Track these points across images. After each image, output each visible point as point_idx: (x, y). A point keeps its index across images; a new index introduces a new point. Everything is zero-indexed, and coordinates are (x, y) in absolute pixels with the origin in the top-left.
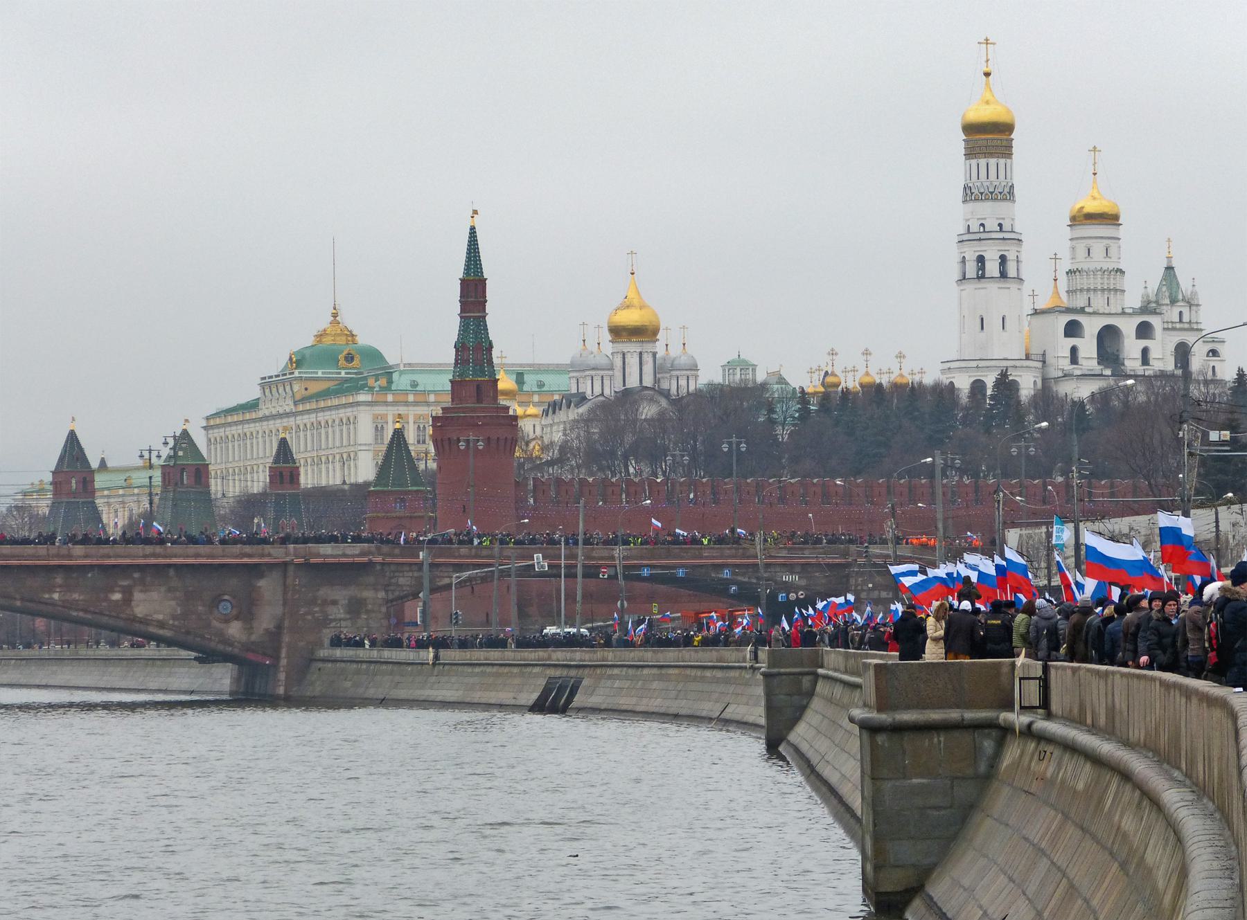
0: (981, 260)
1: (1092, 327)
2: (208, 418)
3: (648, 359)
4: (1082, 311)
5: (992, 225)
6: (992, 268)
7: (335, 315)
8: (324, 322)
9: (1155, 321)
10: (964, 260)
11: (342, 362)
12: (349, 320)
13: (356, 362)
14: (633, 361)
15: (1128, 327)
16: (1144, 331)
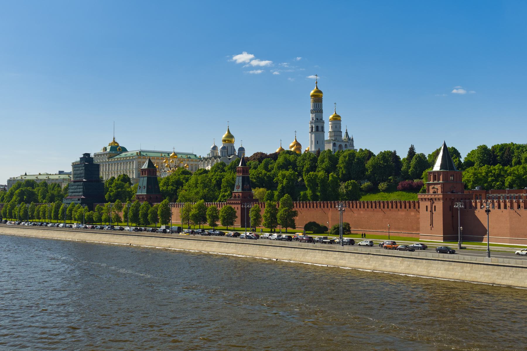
0: (317, 127)
1: (338, 144)
2: (73, 163)
3: (233, 147)
4: (334, 140)
5: (319, 119)
6: (320, 129)
7: (114, 139)
8: (111, 141)
9: (347, 144)
10: (312, 128)
11: (118, 150)
12: (117, 140)
13: (121, 150)
14: (229, 149)
15: (343, 145)
16: (346, 145)
